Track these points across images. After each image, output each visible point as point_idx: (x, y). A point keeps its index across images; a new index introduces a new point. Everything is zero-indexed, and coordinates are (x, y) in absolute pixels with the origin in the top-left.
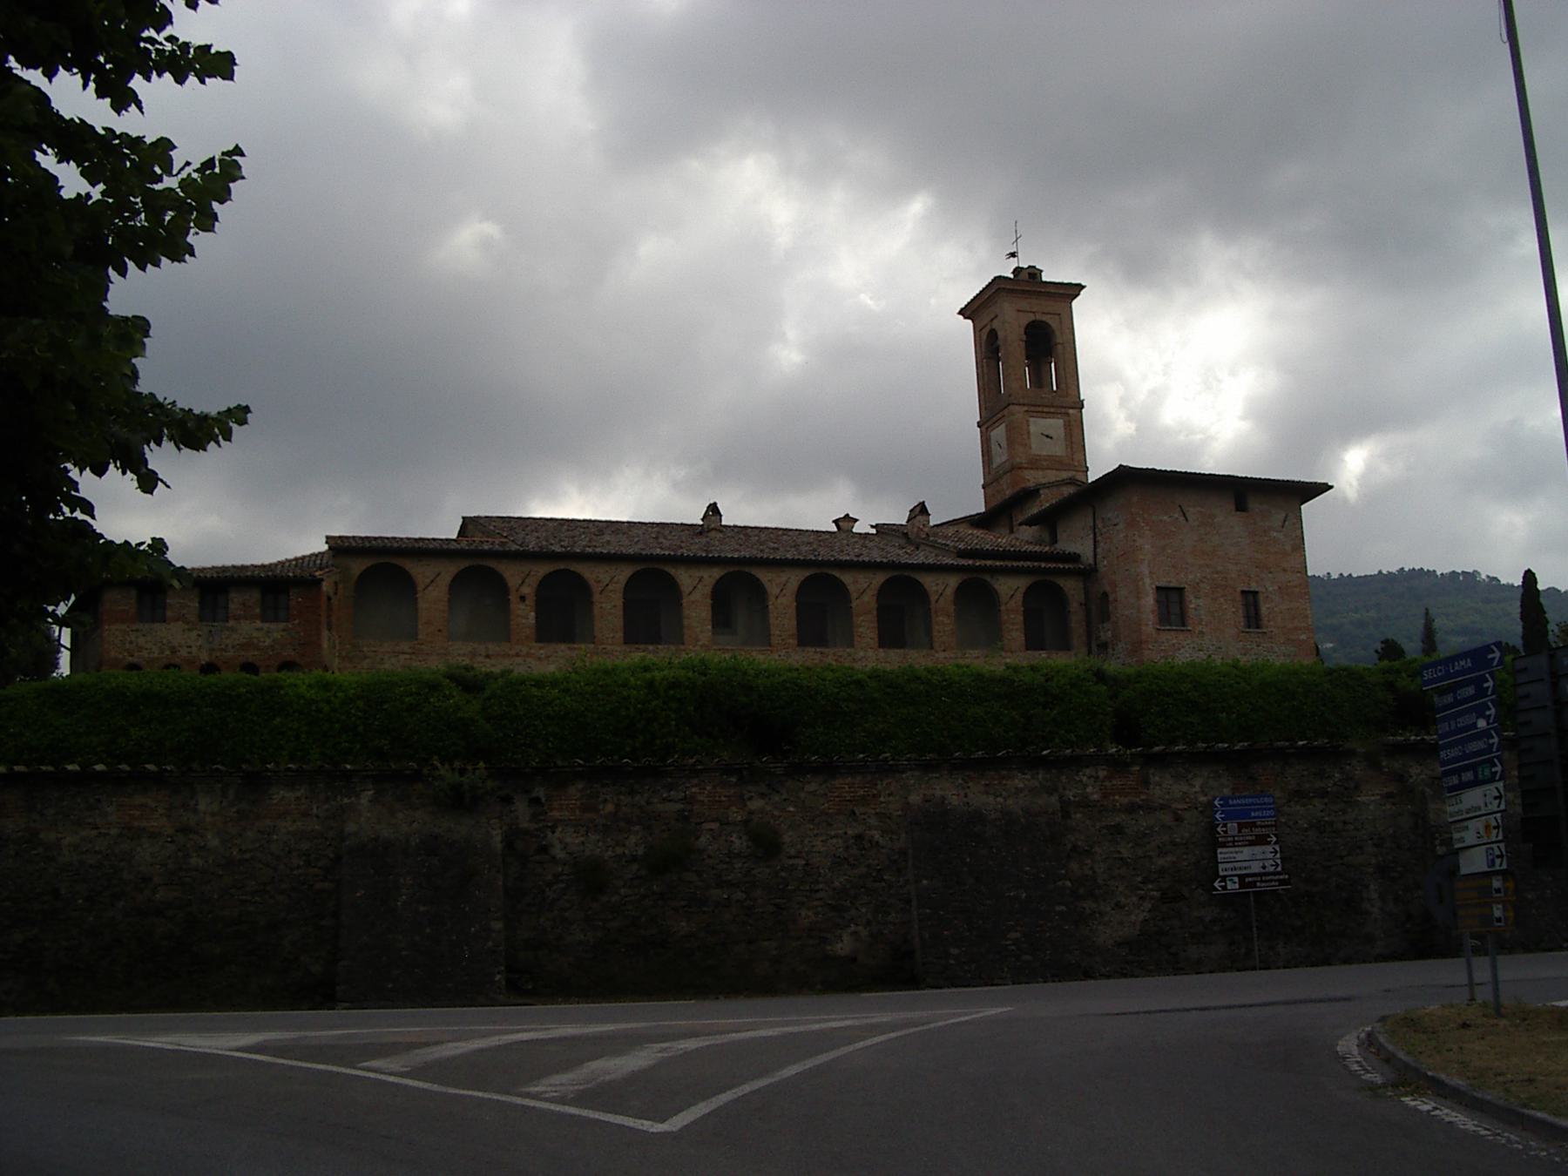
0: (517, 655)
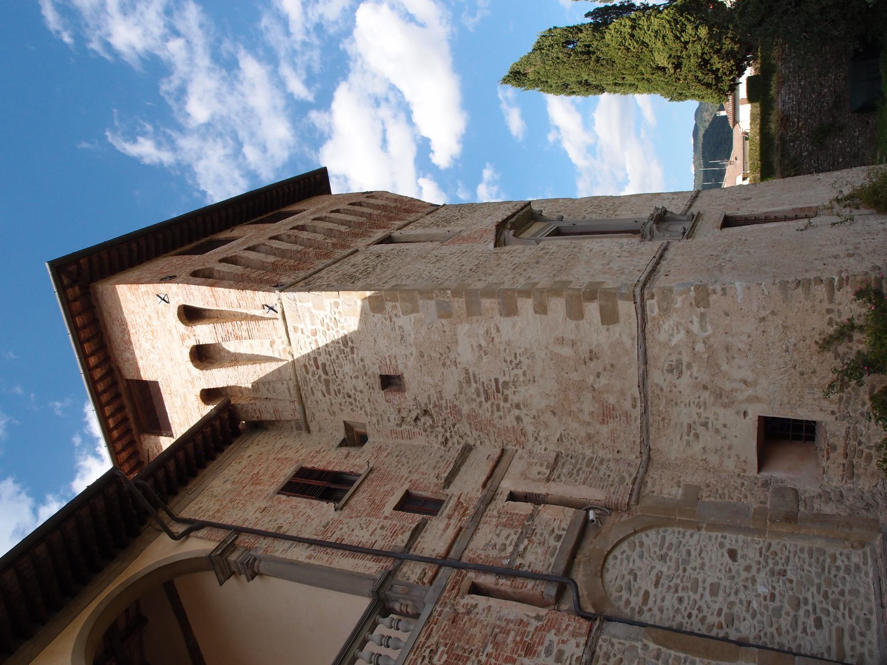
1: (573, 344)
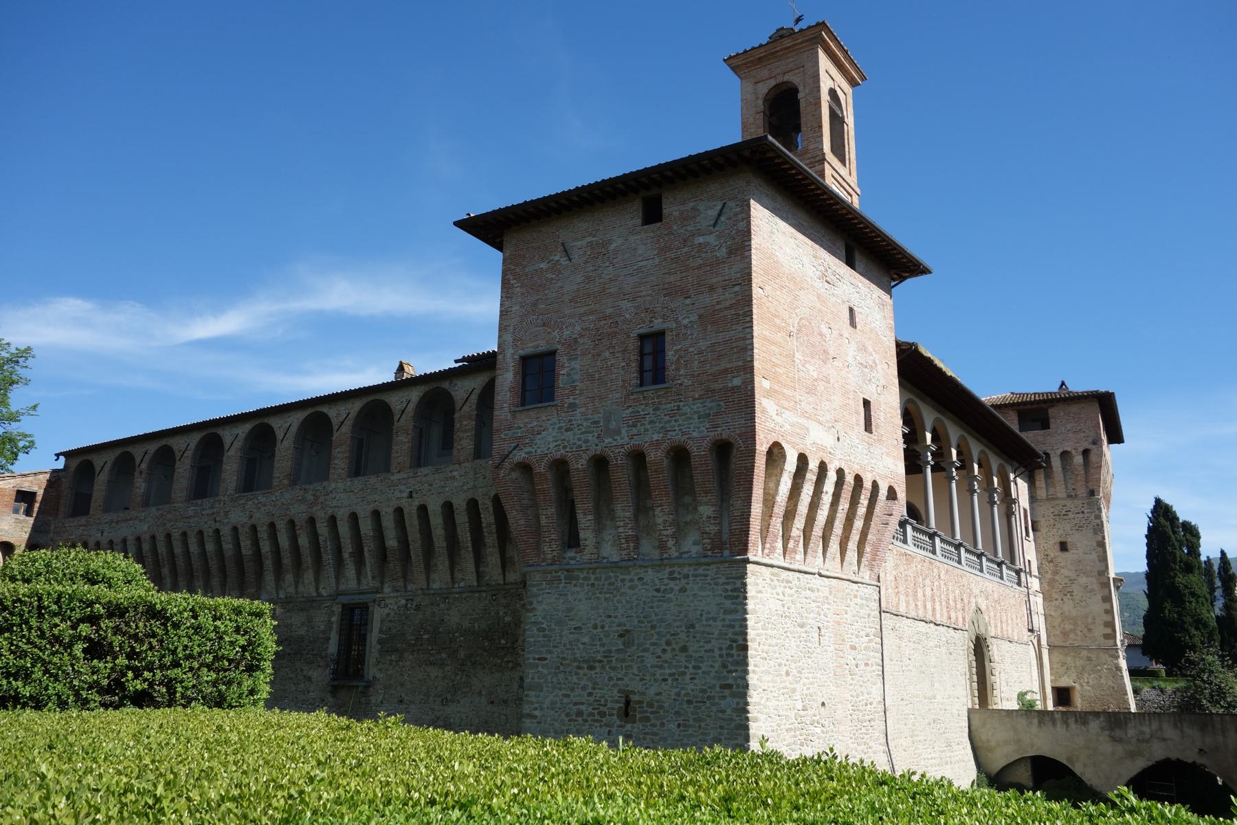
0: (131, 519)
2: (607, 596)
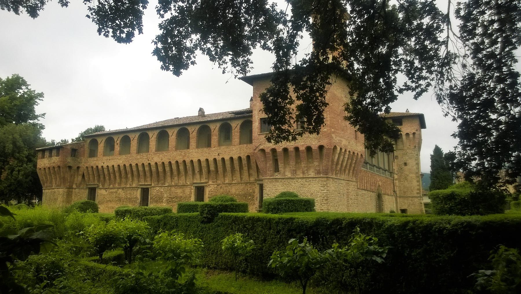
0: (115, 159)
1: (414, 189)
2: (287, 186)
